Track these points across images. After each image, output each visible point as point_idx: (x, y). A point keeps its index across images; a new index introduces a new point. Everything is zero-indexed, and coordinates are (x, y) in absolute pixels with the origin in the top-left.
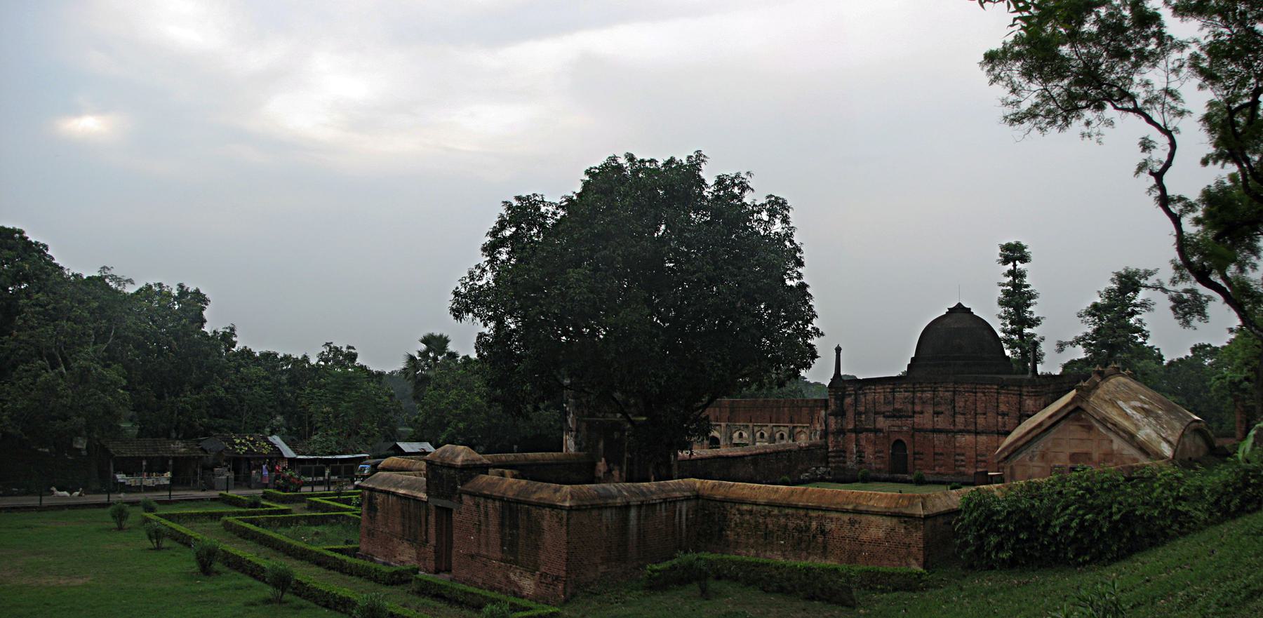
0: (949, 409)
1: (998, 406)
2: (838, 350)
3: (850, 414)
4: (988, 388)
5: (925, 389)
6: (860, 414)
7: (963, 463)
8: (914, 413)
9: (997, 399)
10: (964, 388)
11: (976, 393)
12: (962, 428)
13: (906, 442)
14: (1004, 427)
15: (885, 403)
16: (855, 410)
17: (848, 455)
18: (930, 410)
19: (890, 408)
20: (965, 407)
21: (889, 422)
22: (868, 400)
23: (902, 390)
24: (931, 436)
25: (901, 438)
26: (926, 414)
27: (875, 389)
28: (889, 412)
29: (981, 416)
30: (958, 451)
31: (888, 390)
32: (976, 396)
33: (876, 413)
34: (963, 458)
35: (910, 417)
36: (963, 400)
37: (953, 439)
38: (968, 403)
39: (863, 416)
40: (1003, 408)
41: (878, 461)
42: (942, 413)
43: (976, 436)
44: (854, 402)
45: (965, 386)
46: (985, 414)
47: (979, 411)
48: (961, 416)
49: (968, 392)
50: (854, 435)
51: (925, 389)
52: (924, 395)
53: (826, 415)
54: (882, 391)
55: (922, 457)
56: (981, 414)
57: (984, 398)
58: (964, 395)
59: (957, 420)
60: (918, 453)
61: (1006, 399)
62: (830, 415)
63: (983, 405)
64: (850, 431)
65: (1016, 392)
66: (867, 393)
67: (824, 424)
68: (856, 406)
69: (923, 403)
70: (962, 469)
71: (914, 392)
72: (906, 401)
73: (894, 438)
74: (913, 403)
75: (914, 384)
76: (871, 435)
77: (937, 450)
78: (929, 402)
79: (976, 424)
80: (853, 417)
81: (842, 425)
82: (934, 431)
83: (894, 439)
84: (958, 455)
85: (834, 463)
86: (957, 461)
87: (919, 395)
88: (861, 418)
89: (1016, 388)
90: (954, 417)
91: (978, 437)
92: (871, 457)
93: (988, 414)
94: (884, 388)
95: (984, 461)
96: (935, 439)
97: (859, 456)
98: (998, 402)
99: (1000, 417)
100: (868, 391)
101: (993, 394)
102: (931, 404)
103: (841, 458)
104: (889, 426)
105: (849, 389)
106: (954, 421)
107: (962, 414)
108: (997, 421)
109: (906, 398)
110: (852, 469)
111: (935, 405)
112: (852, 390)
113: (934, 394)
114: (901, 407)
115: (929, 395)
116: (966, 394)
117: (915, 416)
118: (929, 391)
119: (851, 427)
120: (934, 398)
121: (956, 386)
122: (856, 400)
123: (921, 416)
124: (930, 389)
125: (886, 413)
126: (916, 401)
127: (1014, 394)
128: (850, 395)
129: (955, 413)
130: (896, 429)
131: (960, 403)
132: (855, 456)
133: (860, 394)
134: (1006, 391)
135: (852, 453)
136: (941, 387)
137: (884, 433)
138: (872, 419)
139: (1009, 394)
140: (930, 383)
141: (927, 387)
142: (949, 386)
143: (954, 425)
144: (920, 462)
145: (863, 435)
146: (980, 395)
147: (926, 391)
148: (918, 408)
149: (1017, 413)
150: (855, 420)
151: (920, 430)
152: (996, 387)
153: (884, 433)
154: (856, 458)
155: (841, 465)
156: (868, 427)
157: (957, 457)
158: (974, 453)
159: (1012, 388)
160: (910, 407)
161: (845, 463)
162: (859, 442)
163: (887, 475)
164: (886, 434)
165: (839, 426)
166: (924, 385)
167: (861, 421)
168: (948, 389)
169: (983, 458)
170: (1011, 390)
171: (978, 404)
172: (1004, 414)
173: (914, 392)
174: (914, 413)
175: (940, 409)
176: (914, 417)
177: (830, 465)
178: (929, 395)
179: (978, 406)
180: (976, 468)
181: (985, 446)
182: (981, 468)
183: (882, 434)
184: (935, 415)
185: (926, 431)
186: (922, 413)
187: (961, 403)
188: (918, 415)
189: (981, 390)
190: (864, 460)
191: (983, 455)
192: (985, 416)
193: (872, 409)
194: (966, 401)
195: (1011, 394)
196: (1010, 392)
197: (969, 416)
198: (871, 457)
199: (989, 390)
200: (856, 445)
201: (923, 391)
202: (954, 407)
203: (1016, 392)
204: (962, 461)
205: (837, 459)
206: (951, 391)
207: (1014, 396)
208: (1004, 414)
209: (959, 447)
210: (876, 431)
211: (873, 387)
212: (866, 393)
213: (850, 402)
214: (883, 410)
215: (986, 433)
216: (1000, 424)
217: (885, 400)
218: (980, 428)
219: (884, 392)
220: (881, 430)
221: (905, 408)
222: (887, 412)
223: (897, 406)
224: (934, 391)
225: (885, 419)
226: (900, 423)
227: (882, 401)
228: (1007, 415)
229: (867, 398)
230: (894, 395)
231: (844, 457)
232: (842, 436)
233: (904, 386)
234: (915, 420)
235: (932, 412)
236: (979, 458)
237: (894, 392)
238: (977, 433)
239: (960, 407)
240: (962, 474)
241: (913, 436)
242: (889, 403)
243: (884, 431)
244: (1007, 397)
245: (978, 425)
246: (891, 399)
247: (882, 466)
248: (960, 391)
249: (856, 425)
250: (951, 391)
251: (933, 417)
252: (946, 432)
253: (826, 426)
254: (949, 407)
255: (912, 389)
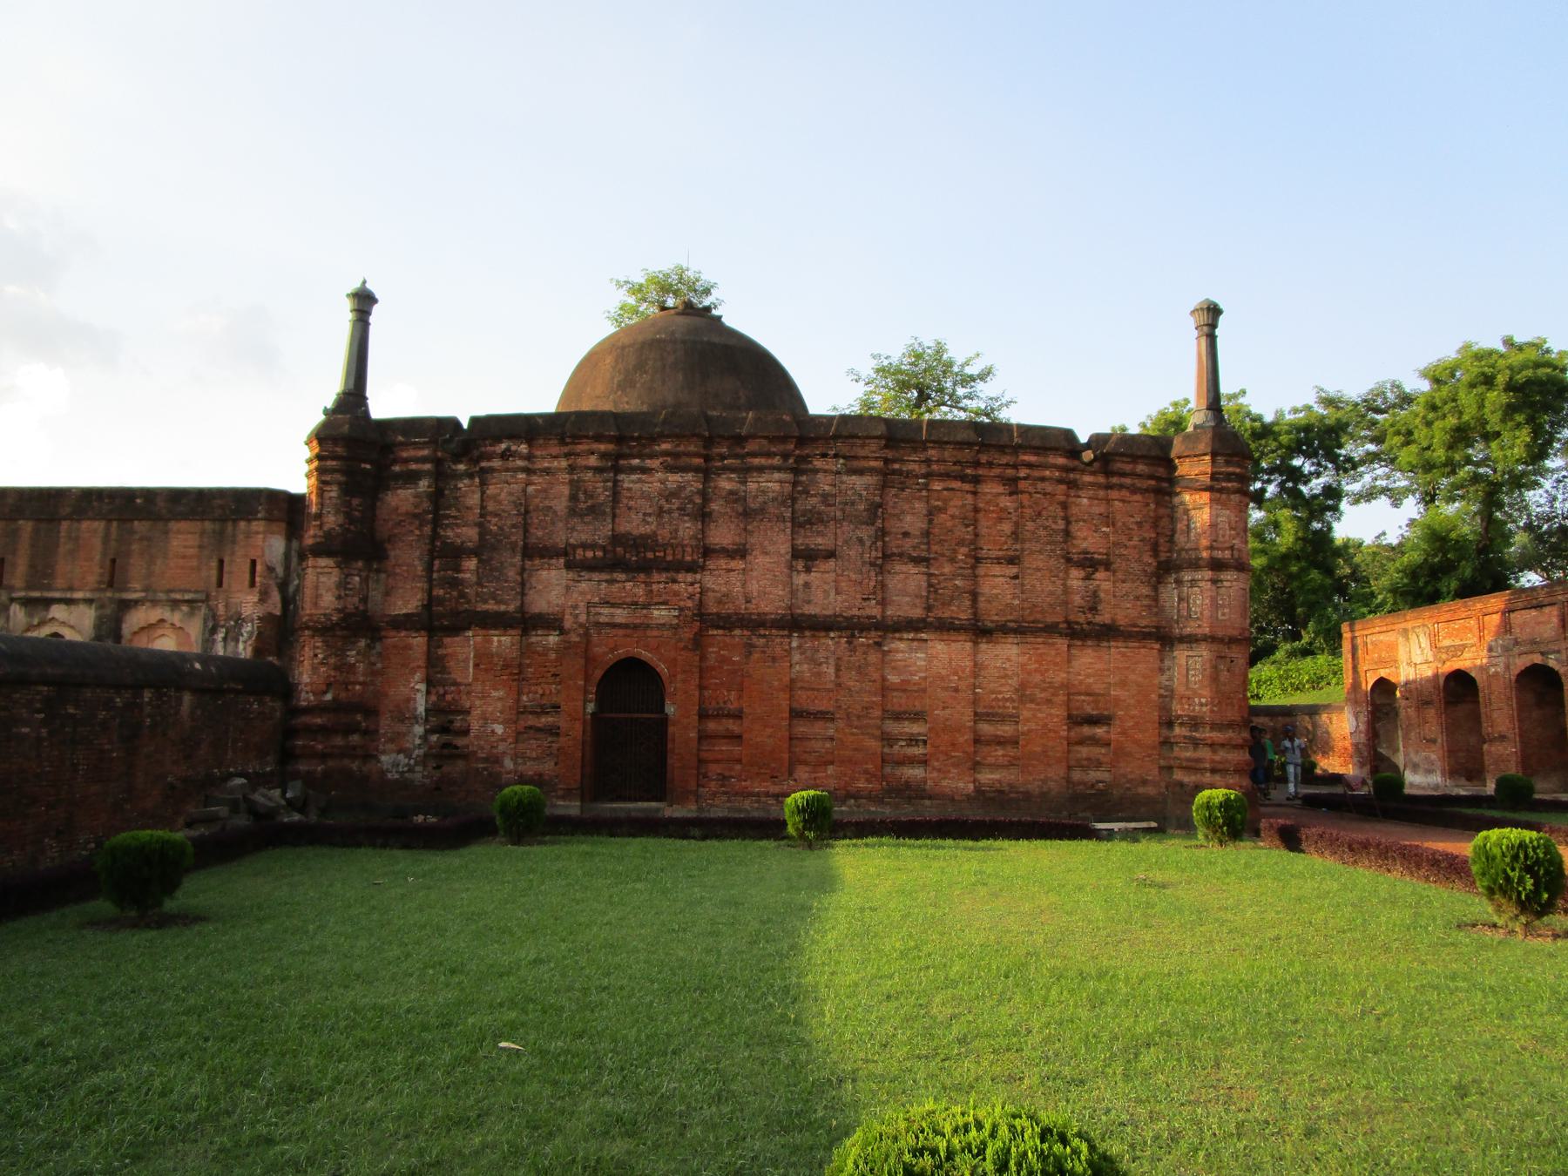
0: (861, 541)
1: (1067, 533)
2: (364, 301)
3: (409, 555)
4: (1030, 466)
5: (756, 461)
6: (454, 554)
7: (918, 751)
8: (708, 552)
9: (1064, 506)
10: (928, 462)
11: (976, 480)
12: (917, 613)
13: (662, 668)
14: (1093, 609)
15: (572, 512)
16: (435, 536)
17: (385, 724)
18: (774, 544)
19: (599, 532)
20: (927, 534)
21: (590, 587)
22: (495, 498)
23: (649, 463)
24: (779, 642)
25: (646, 655)
26: (760, 561)
27: (529, 457)
28: (593, 546)
29: (997, 570)
30: (898, 701)
31: (593, 461)
32: (975, 493)
33: (535, 552)
34: (916, 728)
35: (692, 568)
36: (920, 506)
37: (873, 657)
38: (942, 518)
39: (472, 564)
40: (1088, 540)
41: (532, 747)
42: (831, 554)
43: (976, 643)
44: (426, 505)
45: (933, 453)
46: (1012, 561)
47: (988, 549)
48: (912, 569)
49: (946, 476)
50: (419, 641)
51: (756, 461)
52: (752, 486)
53: (287, 556)
54: (564, 463)
55: (732, 726)
56: (998, 561)
57: (1006, 502)
58: (926, 487)
59: (893, 582)
60: (719, 715)
61: (1098, 509)
62: (318, 551)
63: (1007, 527)
64: (404, 623)
65: (1139, 483)
66: (492, 470)
67: (276, 597)
68: (436, 523)
69: (747, 515)
70: (916, 773)
71: (706, 473)
72: (676, 503)
73: (608, 650)
74: (703, 516)
75: (709, 442)
76: (502, 642)
77: (804, 700)
78: (772, 509)
79: (974, 596)
80: (419, 568)
81: (365, 600)
82: (796, 623)
83: (611, 658)
84: (898, 717)
85: (323, 757)
86: (889, 740)
87: (726, 483)
88: (459, 571)
89: (1141, 468)
90: (881, 570)
91: (983, 646)
92: (499, 729)
93: (1029, 562)
94: (567, 455)
95: (1014, 742)
96: (796, 657)
97: (444, 729)
98: (1068, 523)
99: (1076, 573)
100: (496, 463)
101: (1049, 487)
102: (782, 519)
103: (355, 738)
104: (589, 605)
105: (405, 454)
106: (883, 586)
107: (917, 561)
108: (1067, 590)
109: (670, 495)
110: (403, 785)
111: (800, 523)
112: (424, 460)
113: (795, 484)
114: (647, 529)
115: (771, 484)
116: (937, 486)
117: (711, 564)
118: (779, 469)
119: (407, 602)
120: (794, 500)
121: (890, 454)
122: (438, 498)
123: (733, 564)
124: (777, 461)
125: (580, 552)
126: (714, 506)
127: (1134, 490)
128: (412, 478)
129: (886, 557)
130: (621, 615)
131: (910, 518)
132: (419, 729)
133: (458, 476)
134: (1101, 479)
135: (404, 715)
136: (824, 455)
137: (562, 631)
138: (512, 574)
139: (1109, 487)
140: (784, 439)
141: (769, 455)
142: (862, 453)
143: (883, 603)
144: (725, 747)
145: (464, 649)
146: (990, 489)
147: (761, 469)
148: (723, 534)
149: (1148, 559)
150: (430, 580)
151: (728, 622)
152: (1061, 461)
153: (562, 631)
154: (424, 738)
155: (355, 766)
156: (491, 606)
157: (893, 727)
158: (969, 712)
159: (1128, 468)
160: (687, 529)
161: (369, 756)
162: (444, 670)
163: (572, 808)
164: (575, 638)
165: (353, 602)
166: (751, 446)
167: (455, 583)
168: (855, 464)
169: (1006, 730)
170: (1123, 474)
171: (984, 525)
172: (1090, 564)
173: (706, 473)
174: (708, 552)
175: (821, 542)
176: (703, 568)
177: (303, 767)
178: (771, 484)
179: (983, 531)
180: (976, 766)
181: (1014, 682)
182: (995, 767)
183: (553, 639)
184: (800, 565)
185: (755, 624)
186: (741, 552)
187: (908, 518)
188: (722, 563)
189: (996, 471)
190: (460, 742)
191: (1004, 719)
192: (1013, 570)
193: (517, 537)
194: (931, 514)
195: (1121, 487)
196: (1115, 480)
197: (947, 569)
198: (499, 729)
199: (1036, 473)
200: (429, 682)
201: (745, 472)
202: (883, 533)
203: (1139, 483)
204: (913, 741)
205: (338, 741)
206: (872, 471)
207: (1138, 497)
208: (1090, 564)
209: (903, 688)
210: (527, 622)
211: (523, 448)
212: (483, 471)
213: (406, 507)
214: (560, 537)
215: (1015, 631)
216: (1077, 600)
217: (573, 498)
218: (992, 617)
219: (572, 469)
220: (551, 622)
221: (664, 534)
222: (584, 546)
223: (633, 524)
224: (796, 471)
225: (571, 575)
226: (640, 591)
227: (561, 505)
228: (1107, 565)
229: (491, 490)
230: (616, 482)
231: (366, 732)
232: (362, 643)
233: (665, 446)
234: (709, 581)
235: (785, 549)
236: (986, 728)
237: (617, 470)
238: (980, 631)
239: (906, 534)
240: (912, 792)
241: (698, 643)
242: (594, 511)
243: (568, 623)
244: (1108, 501)
245: (982, 605)
246: (603, 495)
247: (548, 767)
248: (908, 474)
249: (430, 602)
250: (872, 471)
251: (791, 568)
252: (849, 627)
253: (286, 601)
254: (866, 533)
255: (698, 461)
